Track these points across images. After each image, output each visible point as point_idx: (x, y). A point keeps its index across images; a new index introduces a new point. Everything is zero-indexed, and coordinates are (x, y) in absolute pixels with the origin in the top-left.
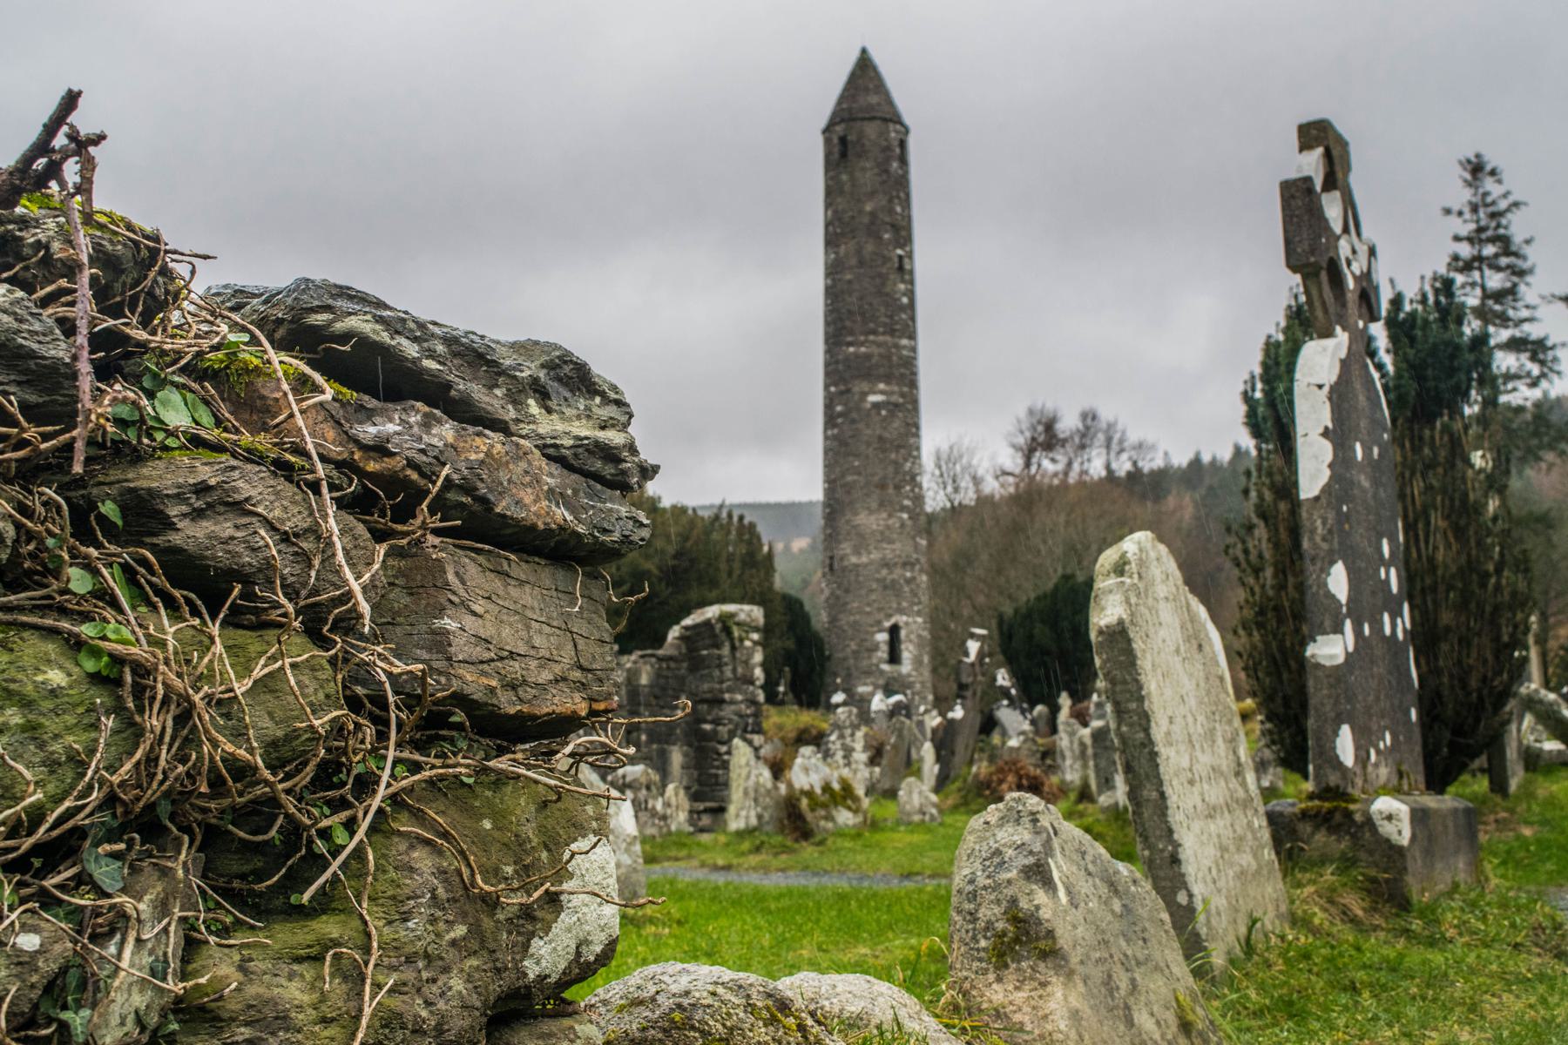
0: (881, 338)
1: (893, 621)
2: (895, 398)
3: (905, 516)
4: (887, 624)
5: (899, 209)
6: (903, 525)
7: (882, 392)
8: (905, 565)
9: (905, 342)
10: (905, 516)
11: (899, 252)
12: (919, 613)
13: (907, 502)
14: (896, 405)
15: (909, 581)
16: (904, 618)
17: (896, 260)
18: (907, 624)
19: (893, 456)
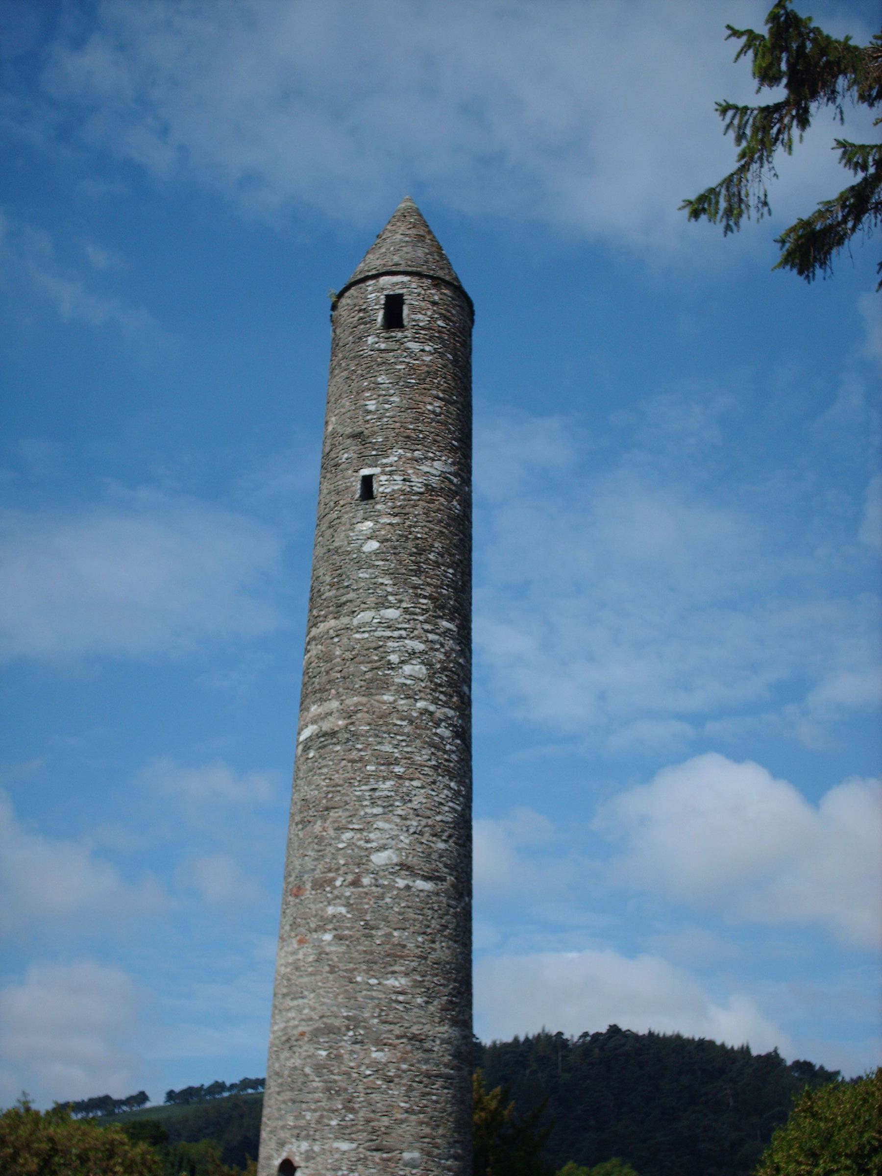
0: (323, 627)
1: (284, 1155)
2: (326, 726)
3: (328, 937)
4: (277, 1162)
5: (372, 406)
6: (321, 955)
7: (314, 722)
8: (316, 1033)
9: (365, 616)
10: (328, 937)
11: (366, 472)
12: (343, 1133)
13: (331, 910)
14: (333, 734)
15: (319, 1068)
16: (305, 1145)
17: (358, 486)
18: (309, 1156)
19: (317, 827)
